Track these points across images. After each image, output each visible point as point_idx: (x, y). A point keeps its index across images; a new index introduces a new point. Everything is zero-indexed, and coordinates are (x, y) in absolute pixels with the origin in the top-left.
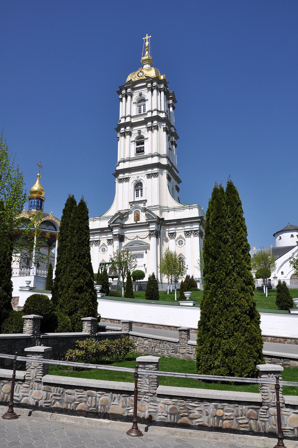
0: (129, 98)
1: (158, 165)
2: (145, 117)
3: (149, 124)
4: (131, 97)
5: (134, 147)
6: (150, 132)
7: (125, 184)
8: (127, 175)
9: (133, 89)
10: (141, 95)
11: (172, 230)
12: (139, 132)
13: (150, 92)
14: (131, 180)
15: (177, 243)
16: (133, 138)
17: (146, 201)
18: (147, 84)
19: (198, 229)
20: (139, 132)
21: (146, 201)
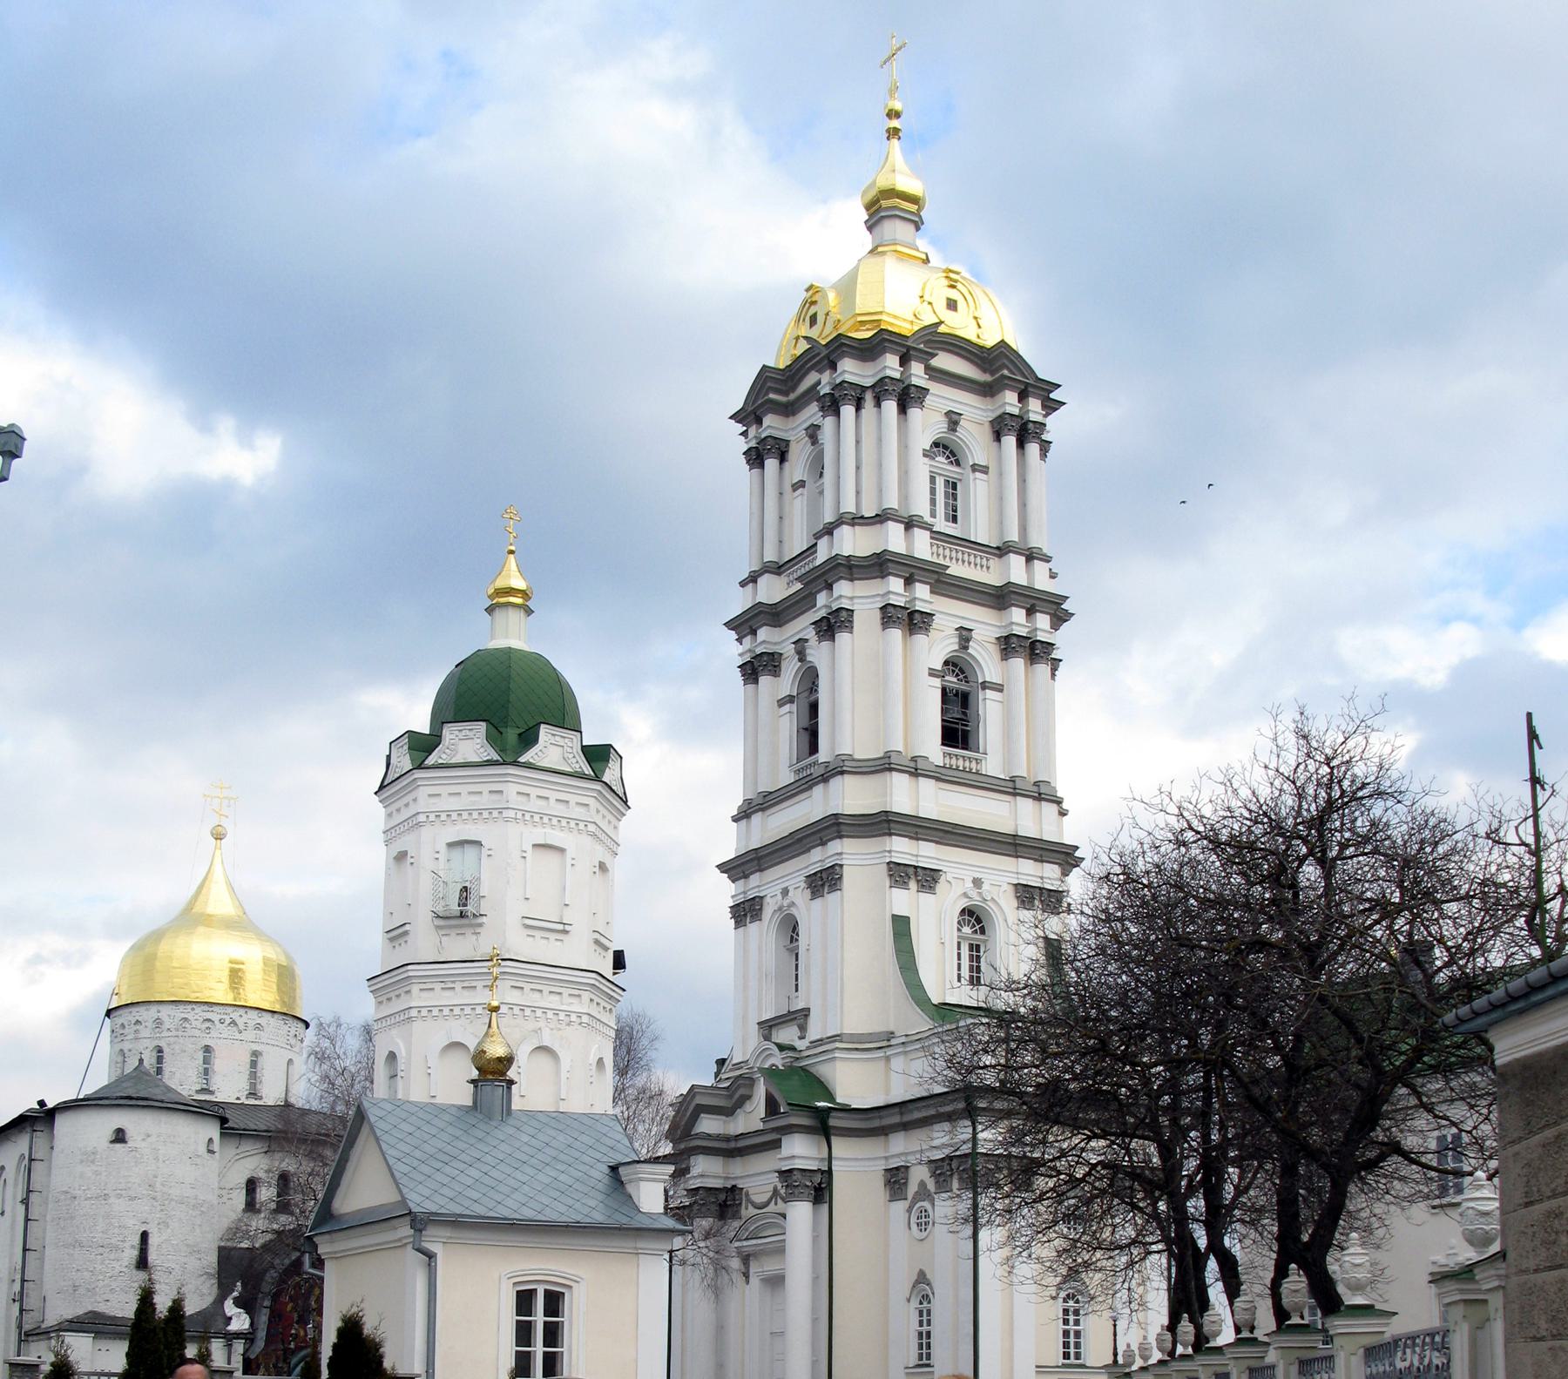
0: (771, 464)
2: (802, 568)
3: (822, 599)
4: (783, 458)
5: (787, 725)
7: (753, 928)
8: (756, 884)
9: (789, 410)
10: (813, 433)
11: (901, 1147)
12: (800, 644)
13: (828, 423)
14: (768, 912)
15: (914, 1220)
17: (805, 1013)
18: (819, 383)
19: (966, 1149)
20: (800, 644)
21: (805, 1013)
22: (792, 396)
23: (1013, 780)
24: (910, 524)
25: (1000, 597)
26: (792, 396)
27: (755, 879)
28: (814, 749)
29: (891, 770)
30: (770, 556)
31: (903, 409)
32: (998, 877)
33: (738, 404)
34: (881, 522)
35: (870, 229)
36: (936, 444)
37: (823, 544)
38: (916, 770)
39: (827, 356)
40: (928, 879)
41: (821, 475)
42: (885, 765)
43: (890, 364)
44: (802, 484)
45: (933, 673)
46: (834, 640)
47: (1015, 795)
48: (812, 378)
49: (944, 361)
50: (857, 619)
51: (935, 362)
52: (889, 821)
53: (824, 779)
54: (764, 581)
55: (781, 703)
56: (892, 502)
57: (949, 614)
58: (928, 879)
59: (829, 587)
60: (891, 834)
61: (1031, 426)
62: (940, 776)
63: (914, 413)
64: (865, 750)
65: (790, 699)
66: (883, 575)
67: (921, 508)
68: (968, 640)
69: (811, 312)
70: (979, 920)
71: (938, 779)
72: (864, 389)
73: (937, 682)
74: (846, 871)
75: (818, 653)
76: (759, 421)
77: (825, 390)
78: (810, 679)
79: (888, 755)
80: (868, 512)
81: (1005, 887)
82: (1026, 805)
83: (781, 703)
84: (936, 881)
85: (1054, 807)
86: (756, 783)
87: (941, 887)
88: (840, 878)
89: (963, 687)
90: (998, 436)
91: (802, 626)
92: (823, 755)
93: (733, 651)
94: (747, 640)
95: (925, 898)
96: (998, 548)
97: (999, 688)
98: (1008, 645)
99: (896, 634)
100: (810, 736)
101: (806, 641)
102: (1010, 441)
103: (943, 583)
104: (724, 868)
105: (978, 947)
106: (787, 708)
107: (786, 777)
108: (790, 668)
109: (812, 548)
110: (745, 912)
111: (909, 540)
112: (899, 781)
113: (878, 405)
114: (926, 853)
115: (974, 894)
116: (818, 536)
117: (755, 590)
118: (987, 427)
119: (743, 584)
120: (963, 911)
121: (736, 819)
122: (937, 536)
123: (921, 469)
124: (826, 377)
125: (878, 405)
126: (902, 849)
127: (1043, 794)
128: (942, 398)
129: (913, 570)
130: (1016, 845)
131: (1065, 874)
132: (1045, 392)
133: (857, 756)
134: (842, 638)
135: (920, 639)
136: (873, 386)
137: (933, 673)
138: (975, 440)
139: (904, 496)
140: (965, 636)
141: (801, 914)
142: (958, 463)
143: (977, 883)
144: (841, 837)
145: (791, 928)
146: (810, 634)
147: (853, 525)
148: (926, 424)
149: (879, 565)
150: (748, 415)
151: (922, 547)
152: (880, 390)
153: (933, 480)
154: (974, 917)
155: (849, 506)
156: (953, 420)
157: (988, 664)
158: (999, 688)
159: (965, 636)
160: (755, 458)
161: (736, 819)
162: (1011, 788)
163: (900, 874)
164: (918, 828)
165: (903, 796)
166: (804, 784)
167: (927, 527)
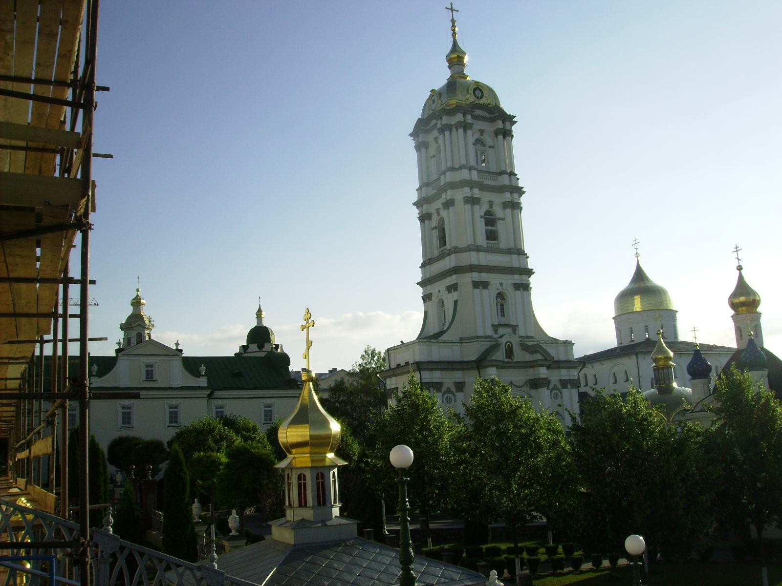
1: (457, 270)
3: (444, 195)
6: (446, 211)
7: (430, 303)
8: (431, 288)
9: (427, 132)
12: (438, 211)
13: (441, 137)
14: (434, 298)
16: (434, 222)
18: (437, 123)
22: (428, 127)
23: (510, 249)
24: (470, 169)
25: (501, 189)
26: (428, 127)
27: (429, 287)
28: (445, 244)
29: (470, 250)
30: (425, 181)
31: (465, 131)
32: (508, 280)
33: (411, 130)
34: (461, 169)
35: (450, 68)
36: (476, 140)
37: (442, 177)
38: (478, 249)
39: (439, 115)
40: (485, 285)
41: (440, 153)
42: (469, 249)
43: (459, 117)
44: (434, 156)
45: (481, 217)
46: (449, 209)
48: (434, 122)
49: (478, 112)
50: (456, 203)
51: (474, 114)
53: (449, 255)
54: (424, 189)
55: (433, 229)
56: (463, 162)
57: (486, 197)
58: (485, 285)
59: (446, 192)
61: (507, 131)
62: (488, 250)
63: (469, 132)
64: (463, 244)
65: (436, 228)
66: (463, 188)
67: (473, 163)
68: (492, 205)
69: (433, 99)
70: (503, 296)
72: (452, 125)
73: (483, 220)
74: (458, 284)
75: (444, 213)
76: (418, 136)
77: (439, 126)
78: (442, 221)
79: (468, 246)
80: (457, 167)
81: (510, 284)
82: (514, 257)
83: (433, 229)
84: (488, 285)
86: (426, 256)
87: (489, 287)
88: (457, 288)
90: (496, 135)
91: (438, 204)
92: (448, 247)
93: (415, 212)
94: (420, 208)
95: (485, 291)
96: (500, 173)
97: (503, 219)
98: (505, 205)
99: (468, 207)
100: (443, 240)
101: (440, 209)
102: (500, 137)
103: (483, 187)
104: (418, 284)
105: (503, 304)
106: (435, 230)
107: (436, 253)
108: (435, 218)
109: (439, 179)
110: (426, 298)
111: (470, 174)
112: (474, 254)
113: (457, 130)
114: (484, 277)
115: (500, 288)
116: (441, 175)
117: (421, 193)
118: (493, 133)
119: (417, 190)
120: (498, 294)
121: (420, 267)
122: (479, 171)
123: (471, 149)
124: (439, 122)
125: (457, 130)
126: (476, 276)
127: (521, 253)
128: (479, 125)
129: (471, 184)
131: (530, 277)
132: (510, 120)
133: (459, 247)
134: (450, 208)
135: (476, 207)
136: (454, 125)
137: (481, 217)
138: (489, 140)
139: (467, 160)
140: (491, 203)
141: (444, 298)
142: (484, 146)
143: (501, 284)
144: (456, 273)
145: (442, 303)
146: (441, 206)
147: (452, 171)
148: (471, 136)
149: (462, 184)
150: (415, 134)
151: (475, 176)
152: (458, 125)
153: (476, 152)
154: (500, 296)
155: (449, 164)
156: (482, 132)
157: (498, 212)
158: (503, 219)
159: (491, 203)
160: (418, 148)
161: (420, 267)
163: (476, 285)
164: (480, 269)
165: (474, 258)
166: (442, 256)
167: (475, 169)
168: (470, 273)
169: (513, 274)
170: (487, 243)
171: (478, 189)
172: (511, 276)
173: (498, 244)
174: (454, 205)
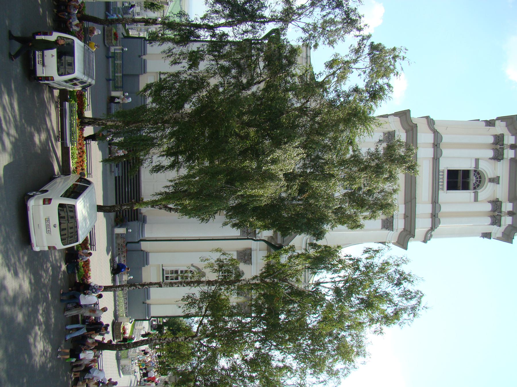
45: (477, 161)
47: (432, 203)
52: (412, 130)
60: (406, 132)
62: (436, 160)
71: (433, 158)
85: (429, 226)
89: (471, 186)
97: (476, 200)
99: (491, 140)
130: (411, 201)
135: (490, 153)
137: (477, 161)
140: (495, 180)
158: (476, 200)
159: (495, 180)
162: (435, 202)
168: (405, 131)
169: (406, 203)
170: (443, 172)
171: (513, 156)
172: (403, 202)
173: (442, 189)
174: (490, 126)
